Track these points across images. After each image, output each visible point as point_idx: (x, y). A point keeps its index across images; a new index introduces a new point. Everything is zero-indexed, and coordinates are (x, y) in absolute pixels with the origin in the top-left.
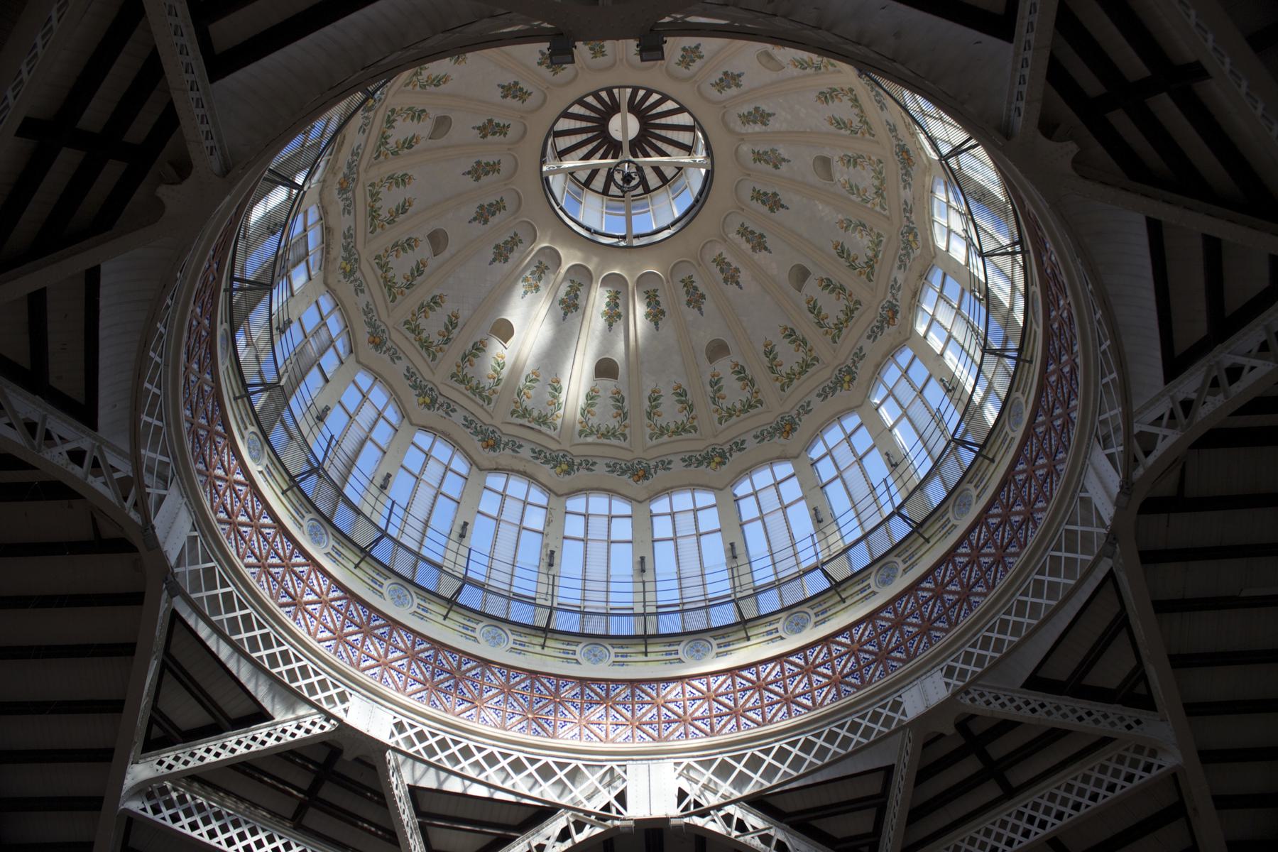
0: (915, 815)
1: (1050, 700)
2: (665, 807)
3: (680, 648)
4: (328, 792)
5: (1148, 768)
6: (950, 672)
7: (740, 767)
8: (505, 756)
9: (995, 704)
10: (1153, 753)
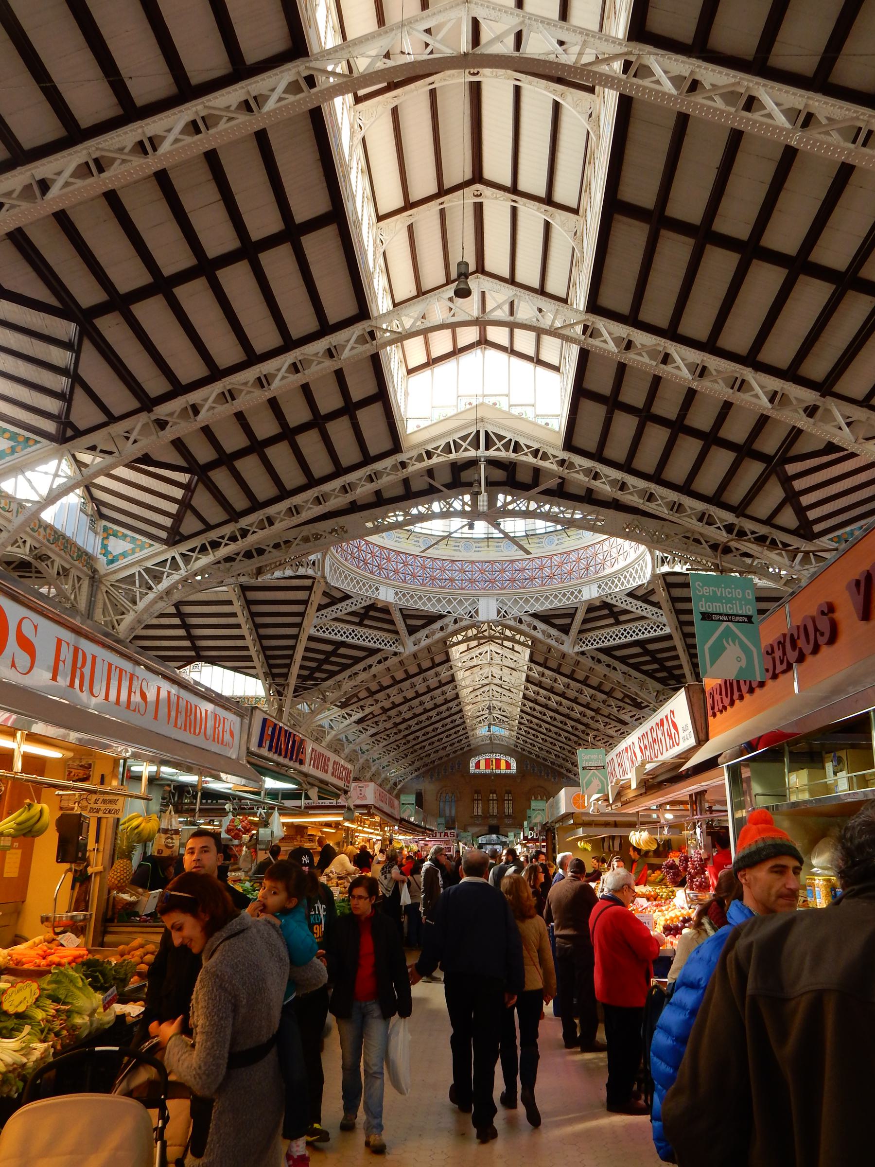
0: (585, 621)
1: (634, 601)
2: (493, 616)
3: (502, 544)
4: (371, 613)
5: (662, 629)
6: (599, 587)
7: (521, 602)
8: (434, 597)
9: (614, 599)
10: (664, 625)
